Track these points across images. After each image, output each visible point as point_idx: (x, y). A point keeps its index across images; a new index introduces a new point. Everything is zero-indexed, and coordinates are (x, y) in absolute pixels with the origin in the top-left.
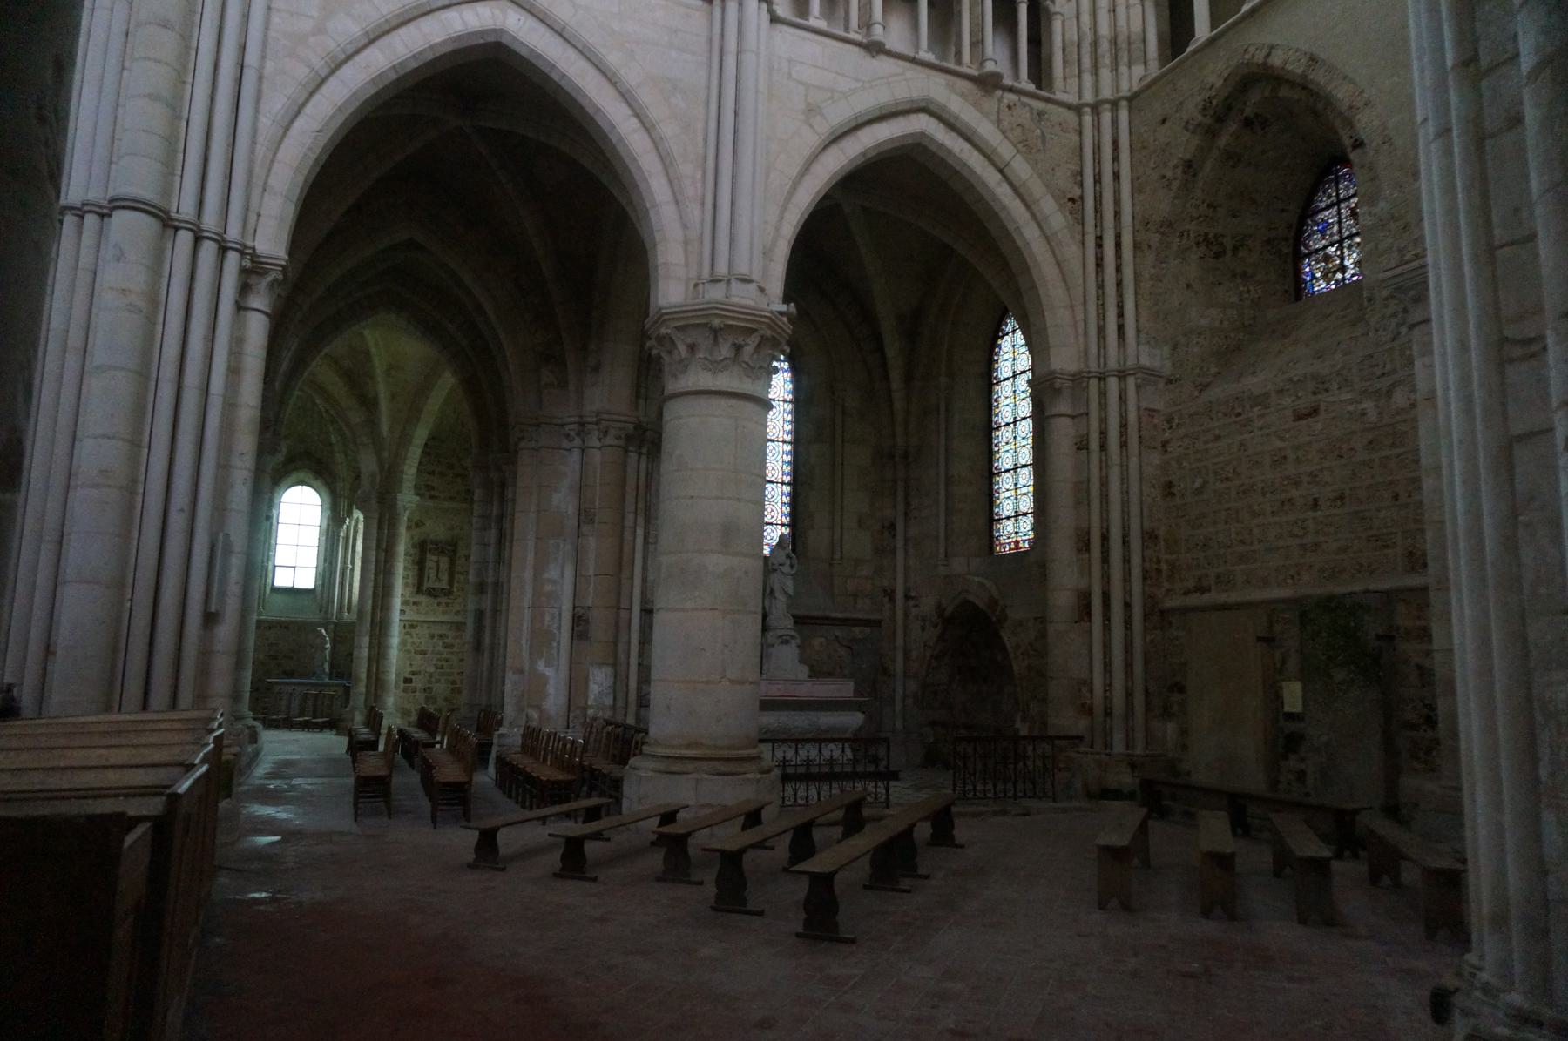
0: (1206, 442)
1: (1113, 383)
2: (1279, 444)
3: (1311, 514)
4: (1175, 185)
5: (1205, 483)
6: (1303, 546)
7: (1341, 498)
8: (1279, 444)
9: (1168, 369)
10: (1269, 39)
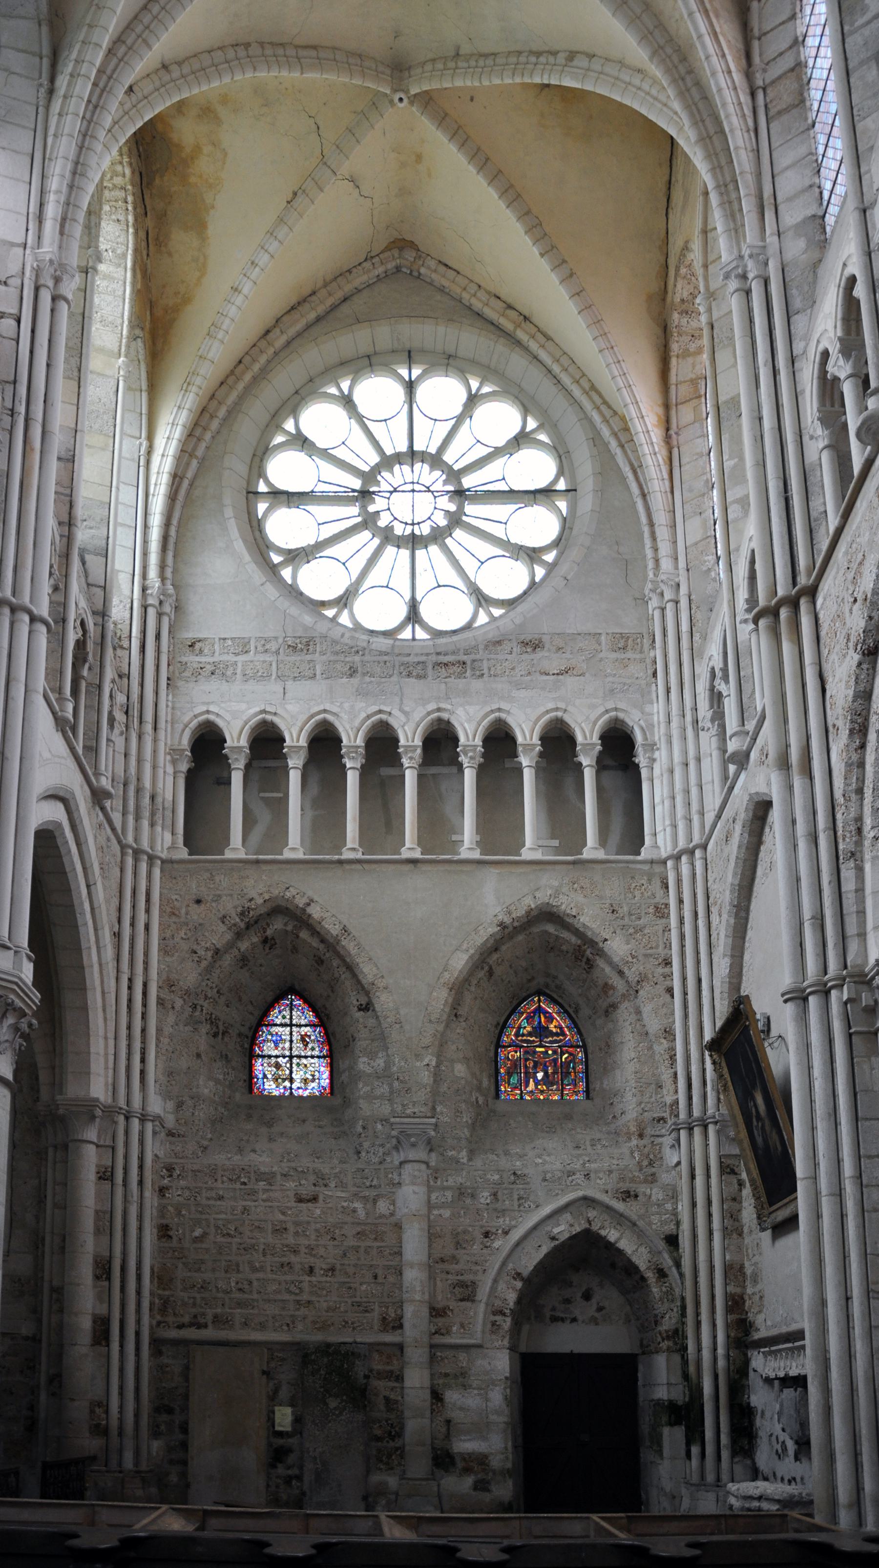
0: (208, 1199)
1: (135, 1123)
2: (282, 1217)
3: (308, 1278)
4: (204, 964)
5: (205, 1235)
6: (298, 1302)
7: (333, 1269)
8: (282, 1217)
9: (170, 1121)
10: (310, 893)
